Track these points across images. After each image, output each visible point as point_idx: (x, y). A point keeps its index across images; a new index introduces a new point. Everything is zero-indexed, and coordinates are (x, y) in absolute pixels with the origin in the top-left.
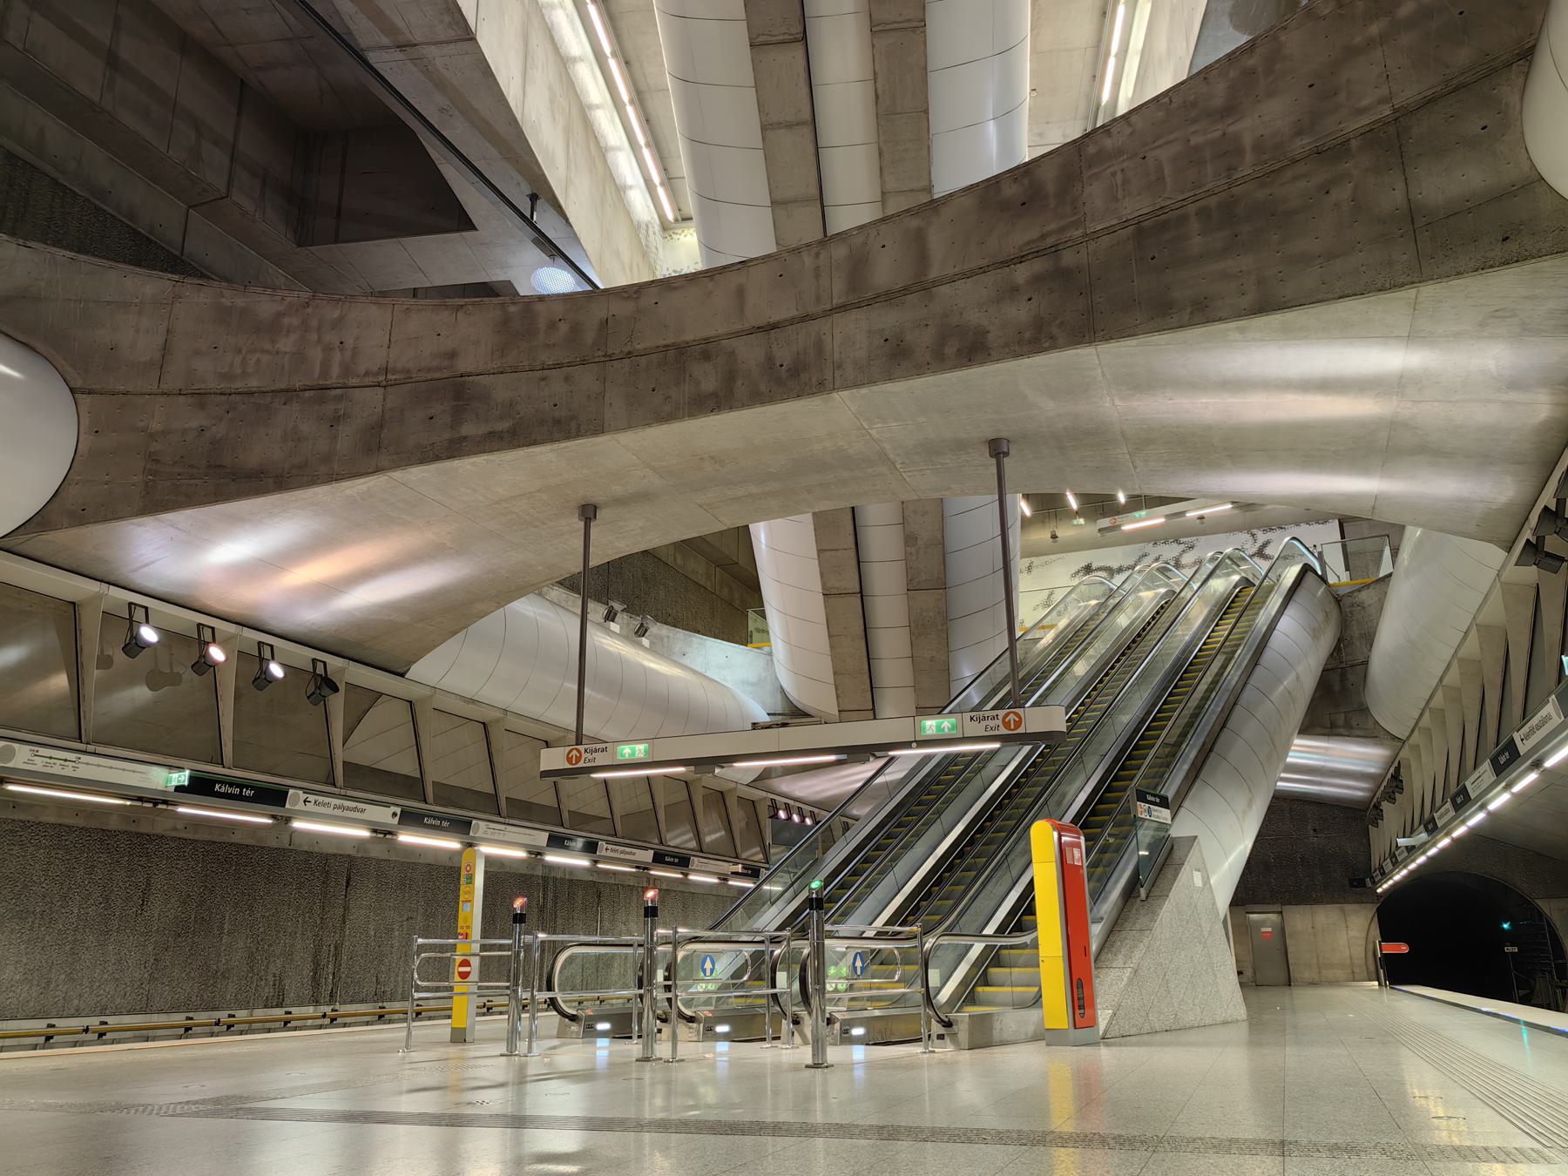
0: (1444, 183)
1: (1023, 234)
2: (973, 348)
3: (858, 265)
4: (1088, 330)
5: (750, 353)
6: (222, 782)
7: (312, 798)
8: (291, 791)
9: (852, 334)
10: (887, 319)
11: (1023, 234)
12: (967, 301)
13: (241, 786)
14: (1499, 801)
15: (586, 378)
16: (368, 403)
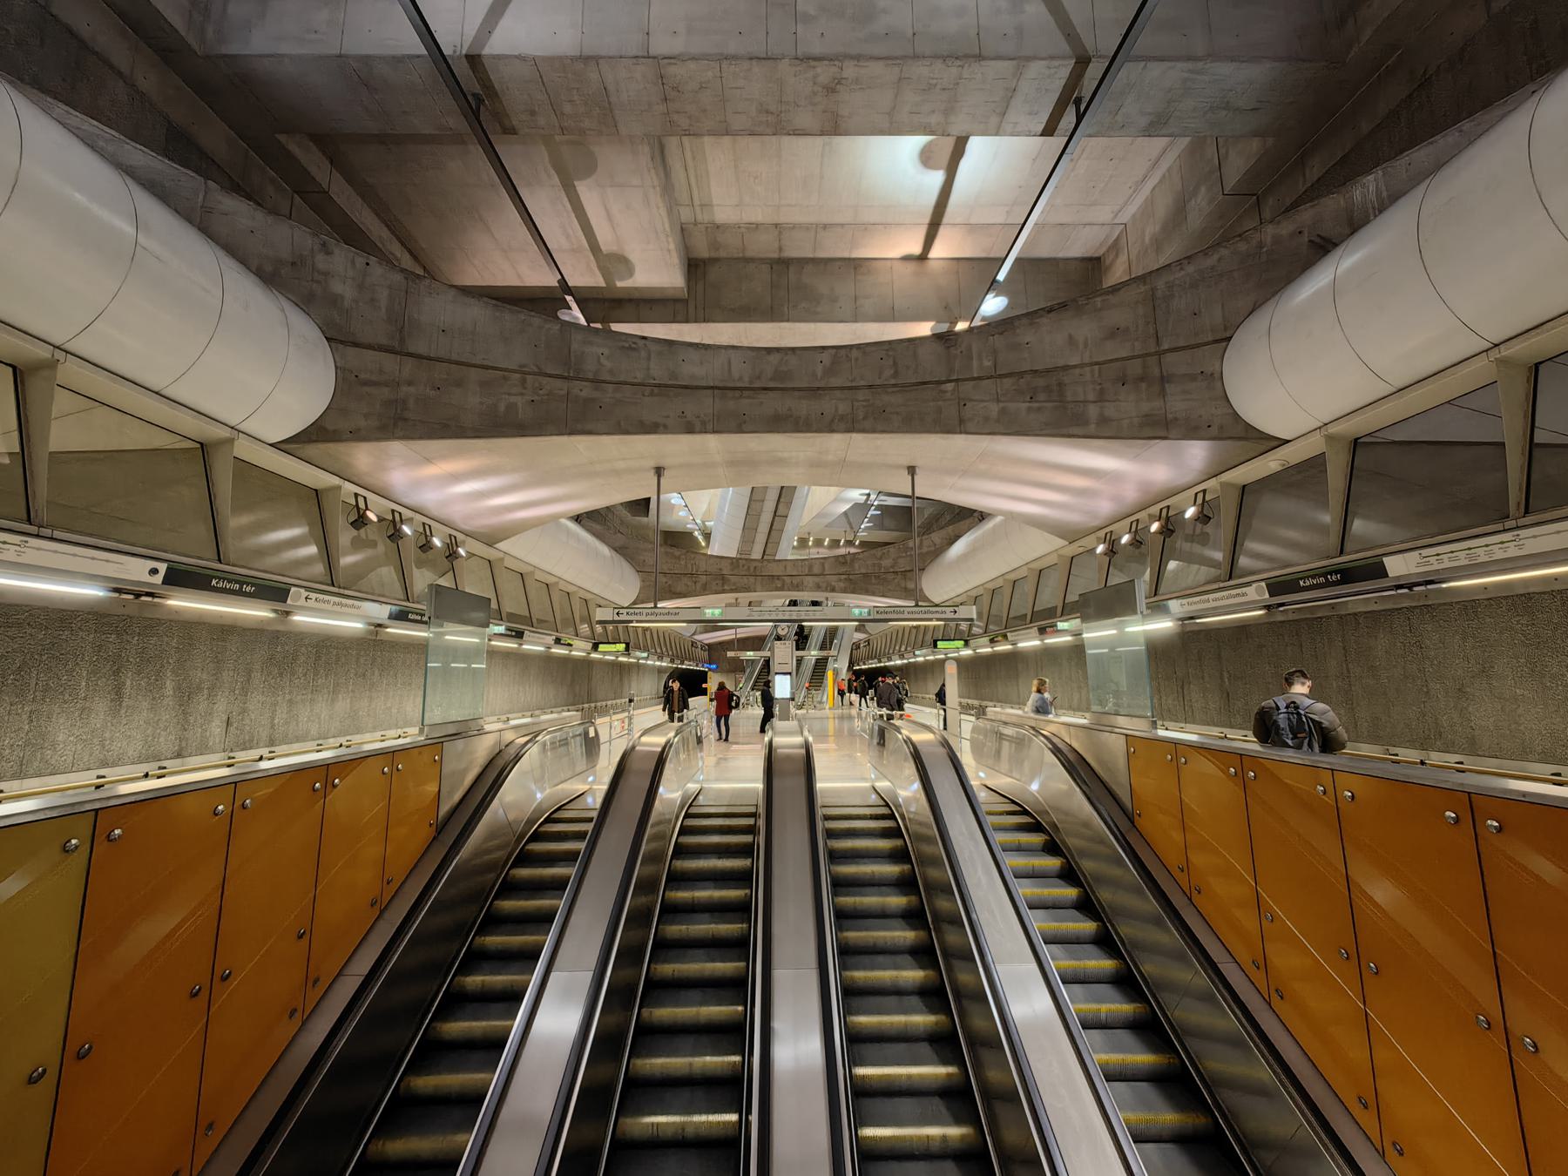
0: (911, 585)
2: (833, 590)
3: (811, 567)
4: (853, 592)
7: (313, 596)
8: (293, 589)
9: (810, 580)
10: (817, 579)
11: (843, 570)
14: (899, 662)
15: (752, 579)
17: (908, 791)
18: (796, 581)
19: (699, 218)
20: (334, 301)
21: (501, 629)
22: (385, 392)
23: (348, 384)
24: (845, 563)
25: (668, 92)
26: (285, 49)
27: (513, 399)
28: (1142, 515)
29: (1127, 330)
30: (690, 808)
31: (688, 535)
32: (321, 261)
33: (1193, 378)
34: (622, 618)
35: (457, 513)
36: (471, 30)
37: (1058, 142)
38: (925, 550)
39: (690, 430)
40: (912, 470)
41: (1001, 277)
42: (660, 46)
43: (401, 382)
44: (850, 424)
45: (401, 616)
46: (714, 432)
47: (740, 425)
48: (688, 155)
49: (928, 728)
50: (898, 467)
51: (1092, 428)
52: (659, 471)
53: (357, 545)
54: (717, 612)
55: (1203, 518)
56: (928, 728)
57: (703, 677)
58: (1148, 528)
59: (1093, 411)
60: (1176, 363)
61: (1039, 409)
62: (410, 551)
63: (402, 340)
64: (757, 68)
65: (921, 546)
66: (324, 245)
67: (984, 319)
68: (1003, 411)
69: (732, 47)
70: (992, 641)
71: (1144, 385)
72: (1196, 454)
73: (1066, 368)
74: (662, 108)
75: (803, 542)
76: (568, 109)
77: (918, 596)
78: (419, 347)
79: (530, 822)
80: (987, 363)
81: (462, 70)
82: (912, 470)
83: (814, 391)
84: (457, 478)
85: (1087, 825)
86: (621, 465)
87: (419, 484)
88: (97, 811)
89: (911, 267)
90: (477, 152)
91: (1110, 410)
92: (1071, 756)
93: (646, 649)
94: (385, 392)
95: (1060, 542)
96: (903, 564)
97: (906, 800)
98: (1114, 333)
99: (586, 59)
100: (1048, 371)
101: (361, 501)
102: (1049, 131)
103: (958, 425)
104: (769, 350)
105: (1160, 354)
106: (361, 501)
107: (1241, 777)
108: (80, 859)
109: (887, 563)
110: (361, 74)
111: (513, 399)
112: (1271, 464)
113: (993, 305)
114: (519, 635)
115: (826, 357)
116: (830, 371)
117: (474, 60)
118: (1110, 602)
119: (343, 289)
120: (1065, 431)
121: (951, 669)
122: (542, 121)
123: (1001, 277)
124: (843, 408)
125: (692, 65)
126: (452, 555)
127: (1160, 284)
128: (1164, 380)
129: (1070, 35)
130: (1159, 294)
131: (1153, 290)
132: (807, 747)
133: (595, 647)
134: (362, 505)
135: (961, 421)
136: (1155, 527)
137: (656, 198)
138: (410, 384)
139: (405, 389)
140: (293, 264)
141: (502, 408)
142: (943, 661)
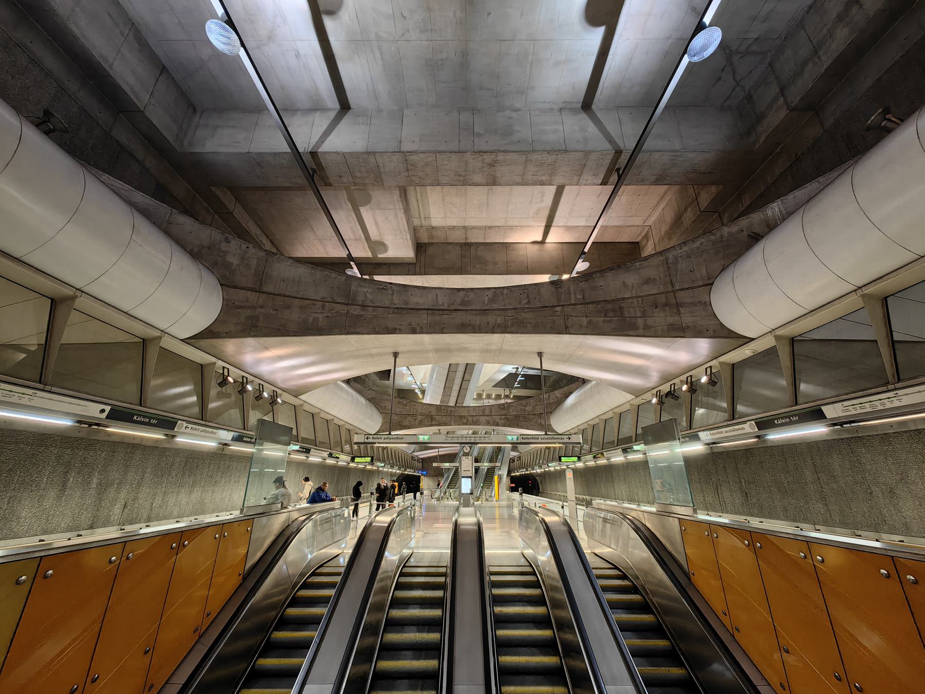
0: (543, 422)
1: (503, 412)
2: (497, 425)
3: (483, 412)
5: (470, 419)
6: (139, 415)
9: (483, 419)
11: (503, 412)
12: (497, 418)
13: (150, 418)
16: (420, 418)
17: (544, 557)
18: (475, 419)
19: (424, 223)
20: (227, 265)
21: (297, 448)
22: (248, 312)
23: (228, 307)
24: (504, 409)
25: (409, 167)
26: (221, 150)
27: (317, 315)
28: (676, 381)
29: (655, 280)
30: (405, 562)
31: (411, 392)
32: (224, 246)
33: (694, 304)
34: (369, 441)
35: (279, 378)
36: (314, 141)
37: (609, 188)
38: (551, 401)
39: (414, 331)
40: (540, 354)
41: (586, 250)
42: (406, 147)
43: (258, 309)
44: (504, 329)
45: (239, 439)
46: (427, 333)
47: (441, 329)
48: (419, 195)
49: (555, 513)
50: (532, 353)
51: (641, 332)
52: (396, 355)
53: (220, 396)
54: (426, 437)
55: (712, 383)
56: (555, 513)
57: (417, 479)
58: (681, 388)
59: (640, 322)
60: (684, 297)
61: (610, 321)
62: (249, 399)
63: (261, 285)
64: (454, 157)
65: (549, 399)
66: (226, 238)
67: (577, 273)
68: (590, 322)
69: (442, 148)
70: (595, 457)
71: (667, 308)
72: (703, 346)
73: (623, 299)
74: (406, 174)
75: (479, 396)
76: (358, 174)
77: (547, 428)
78: (269, 288)
79: (302, 575)
80: (579, 297)
81: (308, 159)
82: (540, 354)
83: (484, 312)
84: (281, 358)
85: (661, 584)
86: (374, 351)
87: (259, 362)
88: (41, 557)
89: (536, 247)
90: (311, 194)
91: (650, 321)
92: (646, 533)
93: (383, 461)
94: (248, 312)
95: (630, 397)
96: (539, 409)
97: (543, 562)
98: (648, 281)
99: (368, 153)
100: (613, 301)
101: (226, 371)
102: (604, 183)
103: (565, 329)
104: (459, 290)
105: (674, 292)
106: (226, 371)
107: (751, 545)
108: (26, 588)
109: (529, 408)
110: (258, 161)
111: (317, 315)
112: (746, 352)
113: (582, 266)
114: (307, 451)
115: (490, 294)
116: (492, 301)
117: (314, 154)
118: (660, 433)
119: (234, 260)
120: (625, 333)
121: (569, 475)
122: (345, 180)
123: (586, 250)
124: (500, 320)
125: (422, 155)
126: (273, 401)
127: (670, 256)
128: (678, 305)
129: (611, 140)
130: (670, 261)
131: (667, 259)
132: (479, 525)
133: (353, 460)
134: (226, 373)
135: (567, 327)
136: (685, 388)
137: (401, 215)
138: (262, 307)
139: (259, 310)
140: (209, 248)
141: (311, 320)
142: (564, 471)
